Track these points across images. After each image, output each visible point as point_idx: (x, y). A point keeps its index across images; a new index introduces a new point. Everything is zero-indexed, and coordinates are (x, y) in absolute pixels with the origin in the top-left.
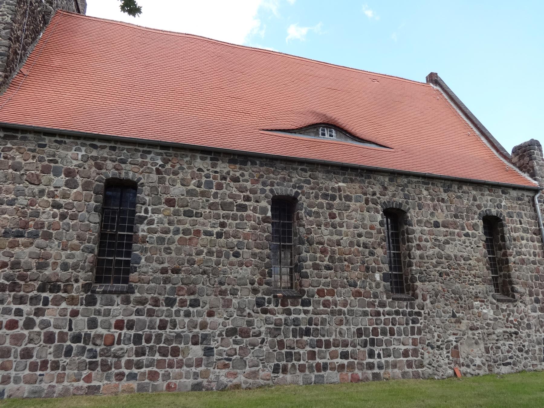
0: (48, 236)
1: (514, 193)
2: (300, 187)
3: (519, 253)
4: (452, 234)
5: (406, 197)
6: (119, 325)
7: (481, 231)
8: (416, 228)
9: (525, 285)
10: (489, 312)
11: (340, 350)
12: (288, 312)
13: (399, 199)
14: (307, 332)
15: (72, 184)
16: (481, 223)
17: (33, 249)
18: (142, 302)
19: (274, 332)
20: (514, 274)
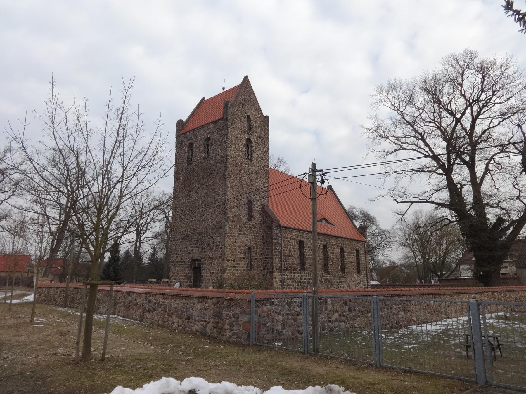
0: (293, 257)
1: (361, 243)
2: (327, 242)
3: (362, 261)
4: (351, 255)
5: (344, 244)
6: (305, 279)
7: (355, 255)
8: (345, 254)
9: (362, 270)
10: (356, 277)
11: (334, 286)
12: (327, 276)
13: (342, 245)
14: (329, 282)
15: (294, 243)
16: (355, 251)
17: (291, 260)
18: (307, 273)
19: (325, 281)
20: (361, 266)
